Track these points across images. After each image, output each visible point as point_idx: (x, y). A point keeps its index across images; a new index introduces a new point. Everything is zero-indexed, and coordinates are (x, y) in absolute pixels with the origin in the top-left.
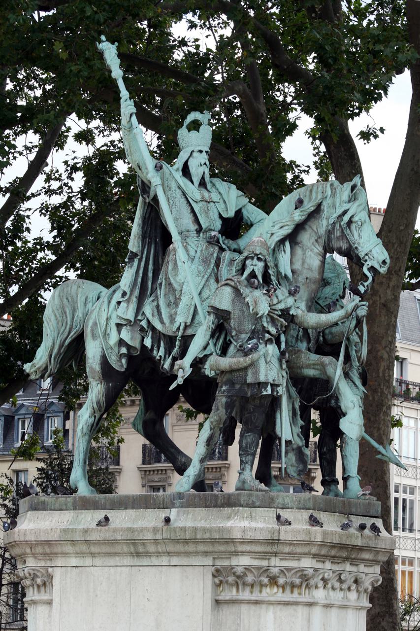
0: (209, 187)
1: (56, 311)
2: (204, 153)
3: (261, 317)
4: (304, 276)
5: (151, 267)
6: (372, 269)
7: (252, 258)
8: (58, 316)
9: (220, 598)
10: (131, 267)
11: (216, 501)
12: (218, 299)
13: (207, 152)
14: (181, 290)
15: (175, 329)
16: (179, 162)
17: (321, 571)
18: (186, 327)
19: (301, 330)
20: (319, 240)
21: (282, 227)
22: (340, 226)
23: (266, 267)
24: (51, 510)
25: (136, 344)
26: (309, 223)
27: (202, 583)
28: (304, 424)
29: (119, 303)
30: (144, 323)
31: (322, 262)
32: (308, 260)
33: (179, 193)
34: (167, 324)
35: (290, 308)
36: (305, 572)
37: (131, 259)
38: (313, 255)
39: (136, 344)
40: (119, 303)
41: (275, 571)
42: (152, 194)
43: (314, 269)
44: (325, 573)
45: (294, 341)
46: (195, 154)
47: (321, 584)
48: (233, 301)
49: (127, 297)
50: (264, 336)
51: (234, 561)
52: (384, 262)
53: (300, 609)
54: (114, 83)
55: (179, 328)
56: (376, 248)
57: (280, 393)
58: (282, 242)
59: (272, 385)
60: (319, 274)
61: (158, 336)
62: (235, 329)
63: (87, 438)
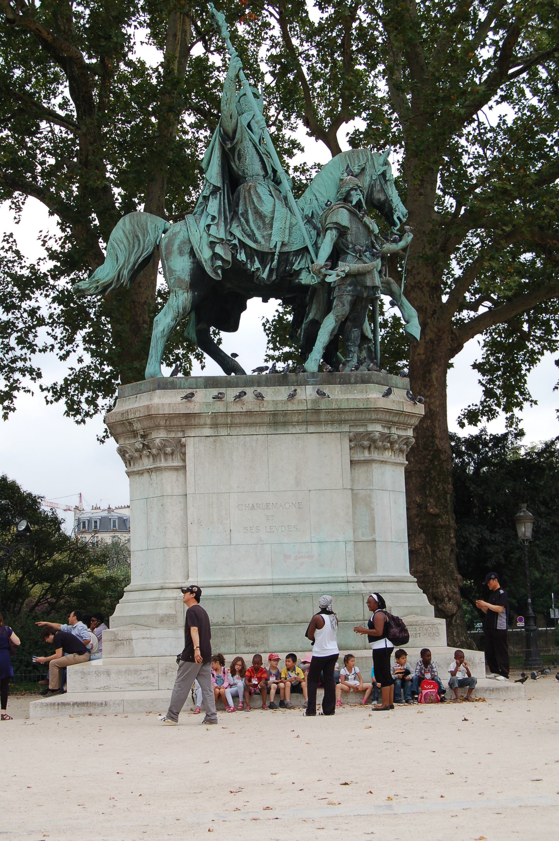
1: (128, 235)
5: (226, 201)
6: (399, 218)
7: (356, 190)
8: (130, 239)
9: (356, 458)
10: (216, 198)
11: (350, 380)
12: (339, 216)
14: (273, 218)
15: (272, 247)
18: (283, 244)
22: (380, 182)
24: (180, 388)
25: (229, 258)
27: (339, 447)
29: (209, 226)
30: (236, 242)
33: (251, 145)
34: (263, 242)
39: (229, 258)
40: (209, 226)
42: (236, 140)
48: (350, 220)
49: (216, 221)
51: (371, 428)
55: (275, 246)
61: (251, 253)
62: (352, 243)
63: (165, 339)
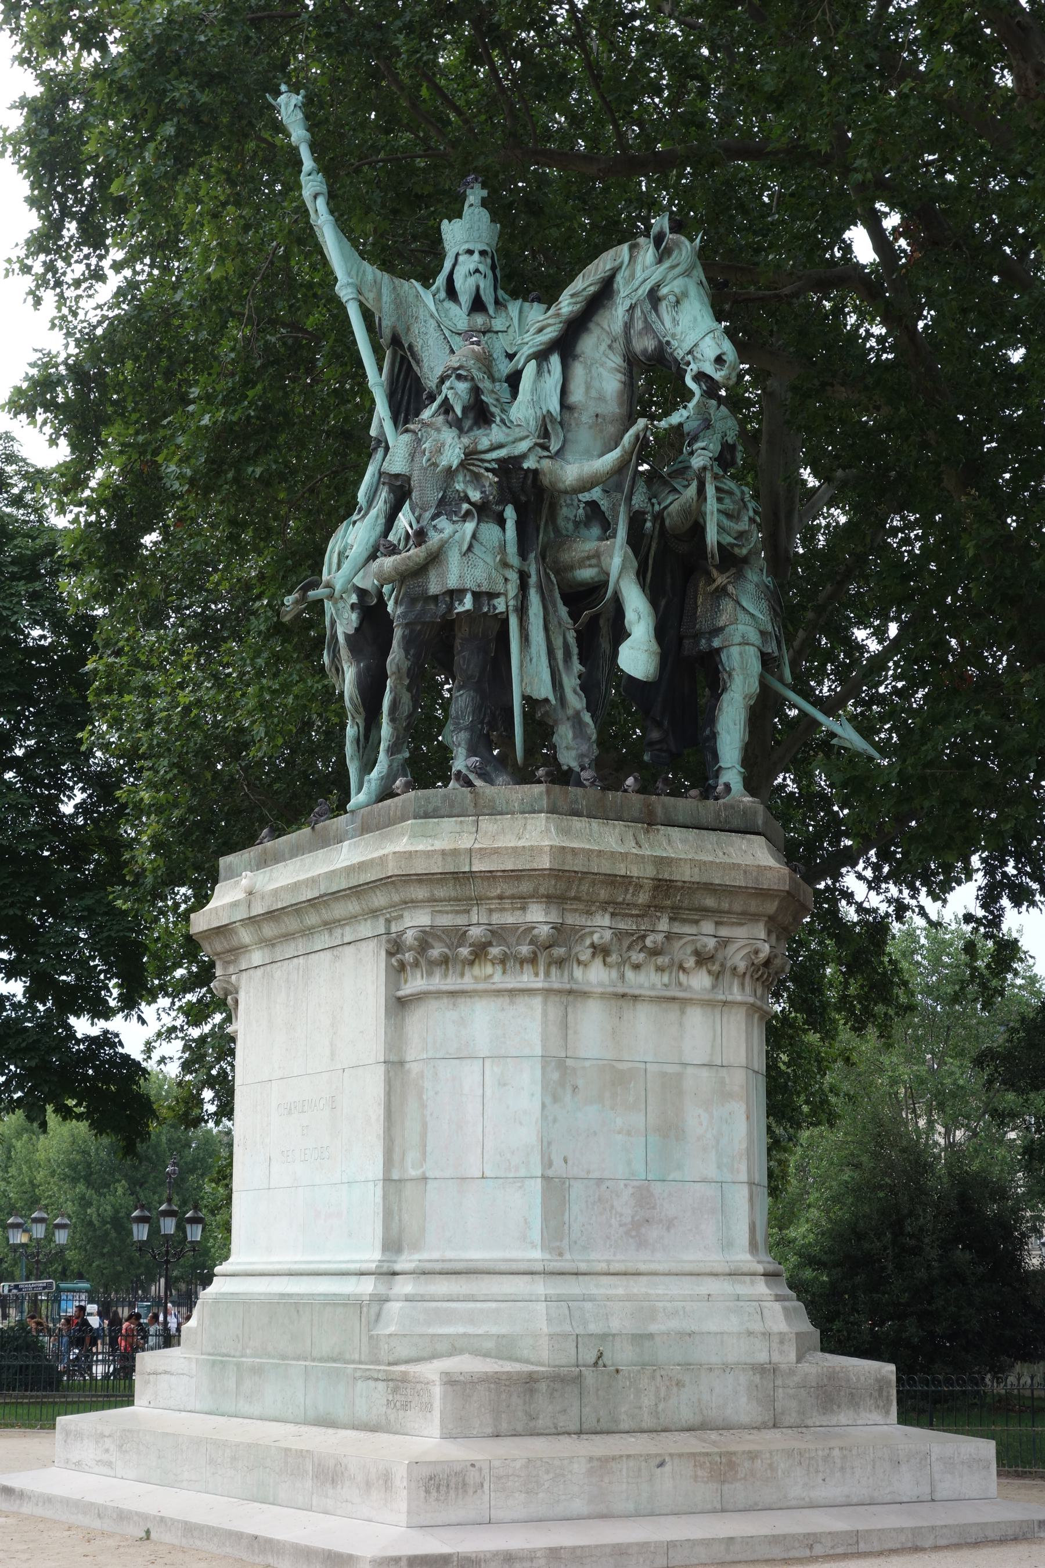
0: (491, 309)
2: (476, 256)
3: (450, 473)
4: (591, 411)
6: (701, 377)
7: (449, 377)
9: (401, 993)
13: (483, 253)
16: (441, 280)
17: (587, 930)
19: (582, 505)
20: (615, 345)
21: (540, 330)
22: (642, 312)
23: (476, 391)
26: (596, 318)
28: (583, 669)
31: (624, 383)
32: (596, 384)
33: (432, 323)
35: (524, 456)
36: (535, 932)
37: (375, 449)
38: (605, 373)
41: (475, 932)
43: (608, 398)
44: (592, 933)
45: (571, 526)
46: (461, 259)
47: (585, 955)
50: (460, 508)
52: (719, 360)
53: (537, 1002)
54: (294, 152)
56: (707, 339)
57: (501, 608)
58: (541, 356)
59: (476, 596)
60: (621, 405)
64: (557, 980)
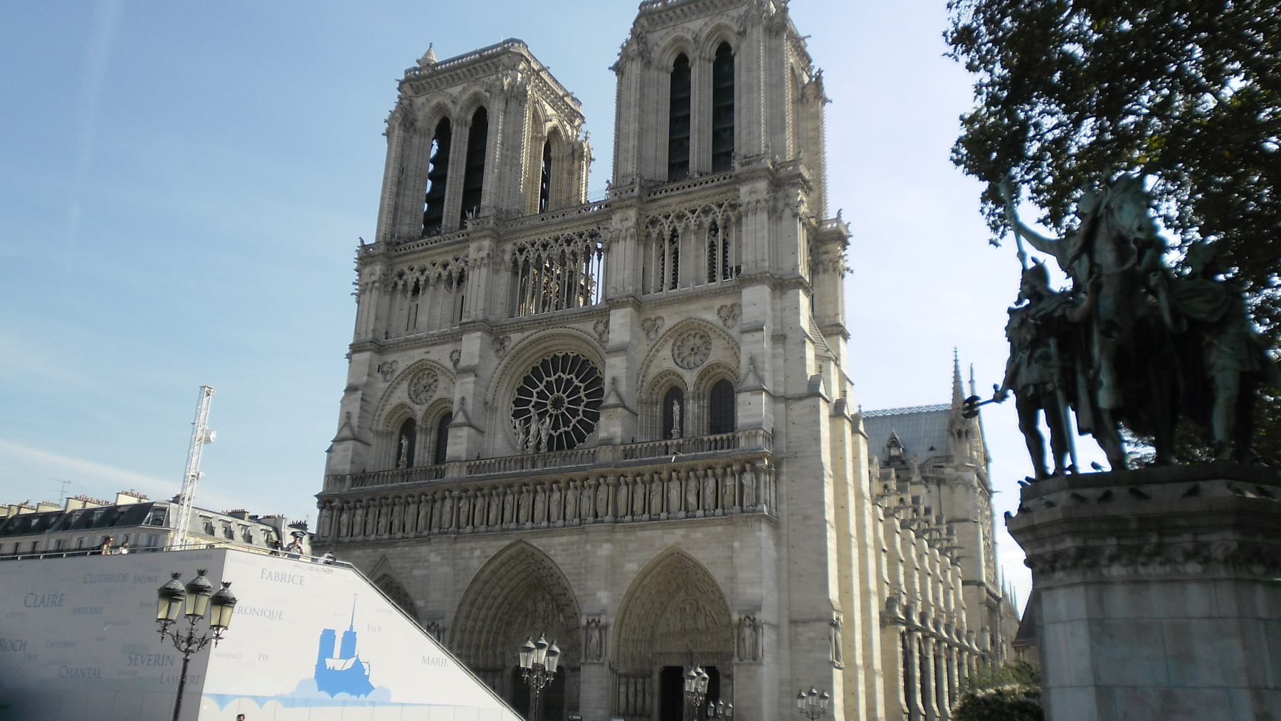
35: (1054, 311)
59: (1036, 386)
64: (1090, 576)
